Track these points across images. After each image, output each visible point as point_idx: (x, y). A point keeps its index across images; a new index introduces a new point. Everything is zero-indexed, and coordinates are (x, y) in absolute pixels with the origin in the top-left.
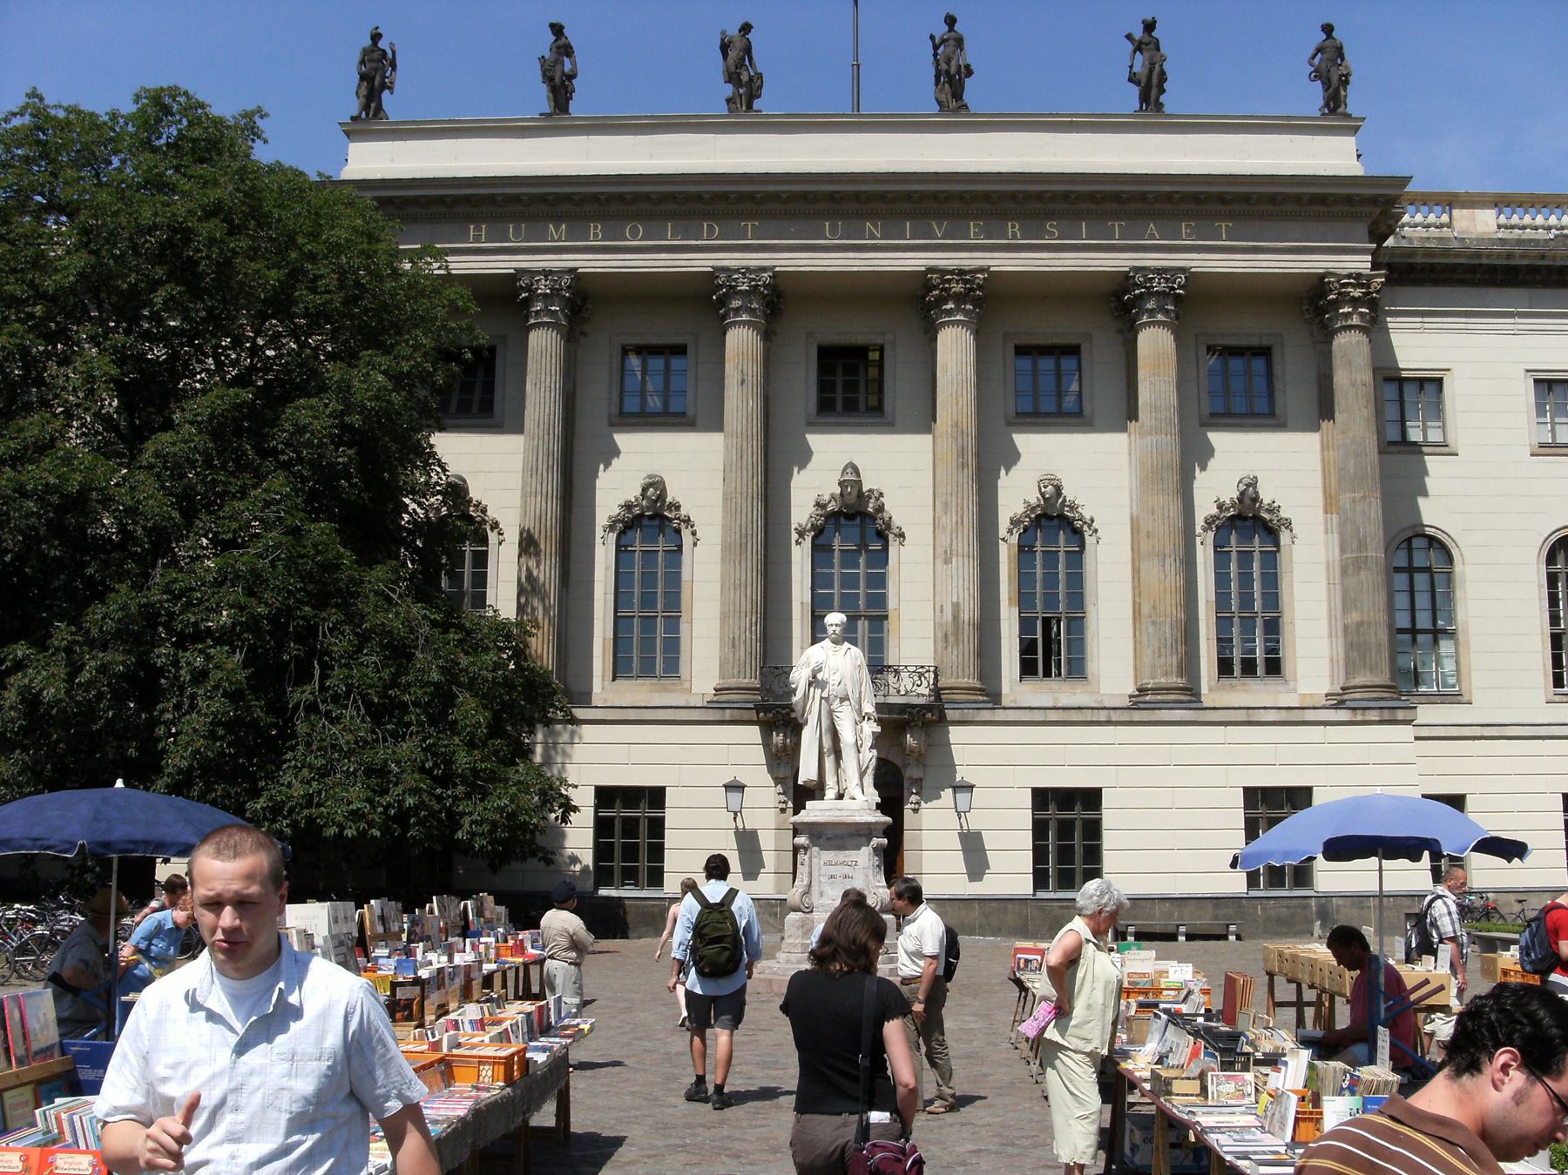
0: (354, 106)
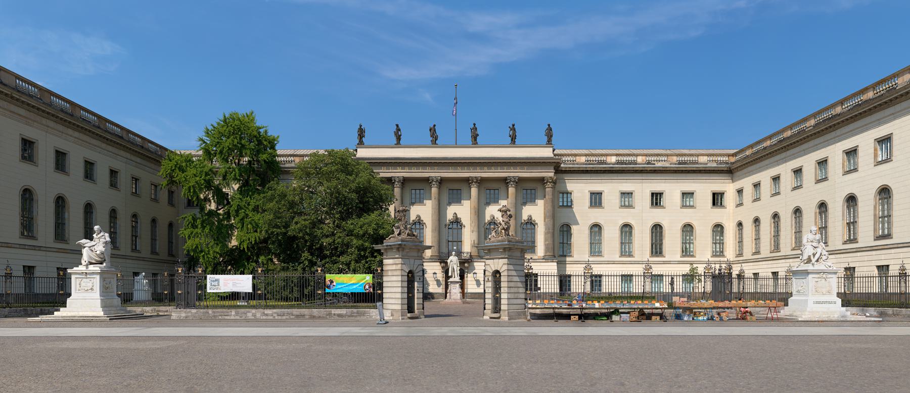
0: (358, 141)
